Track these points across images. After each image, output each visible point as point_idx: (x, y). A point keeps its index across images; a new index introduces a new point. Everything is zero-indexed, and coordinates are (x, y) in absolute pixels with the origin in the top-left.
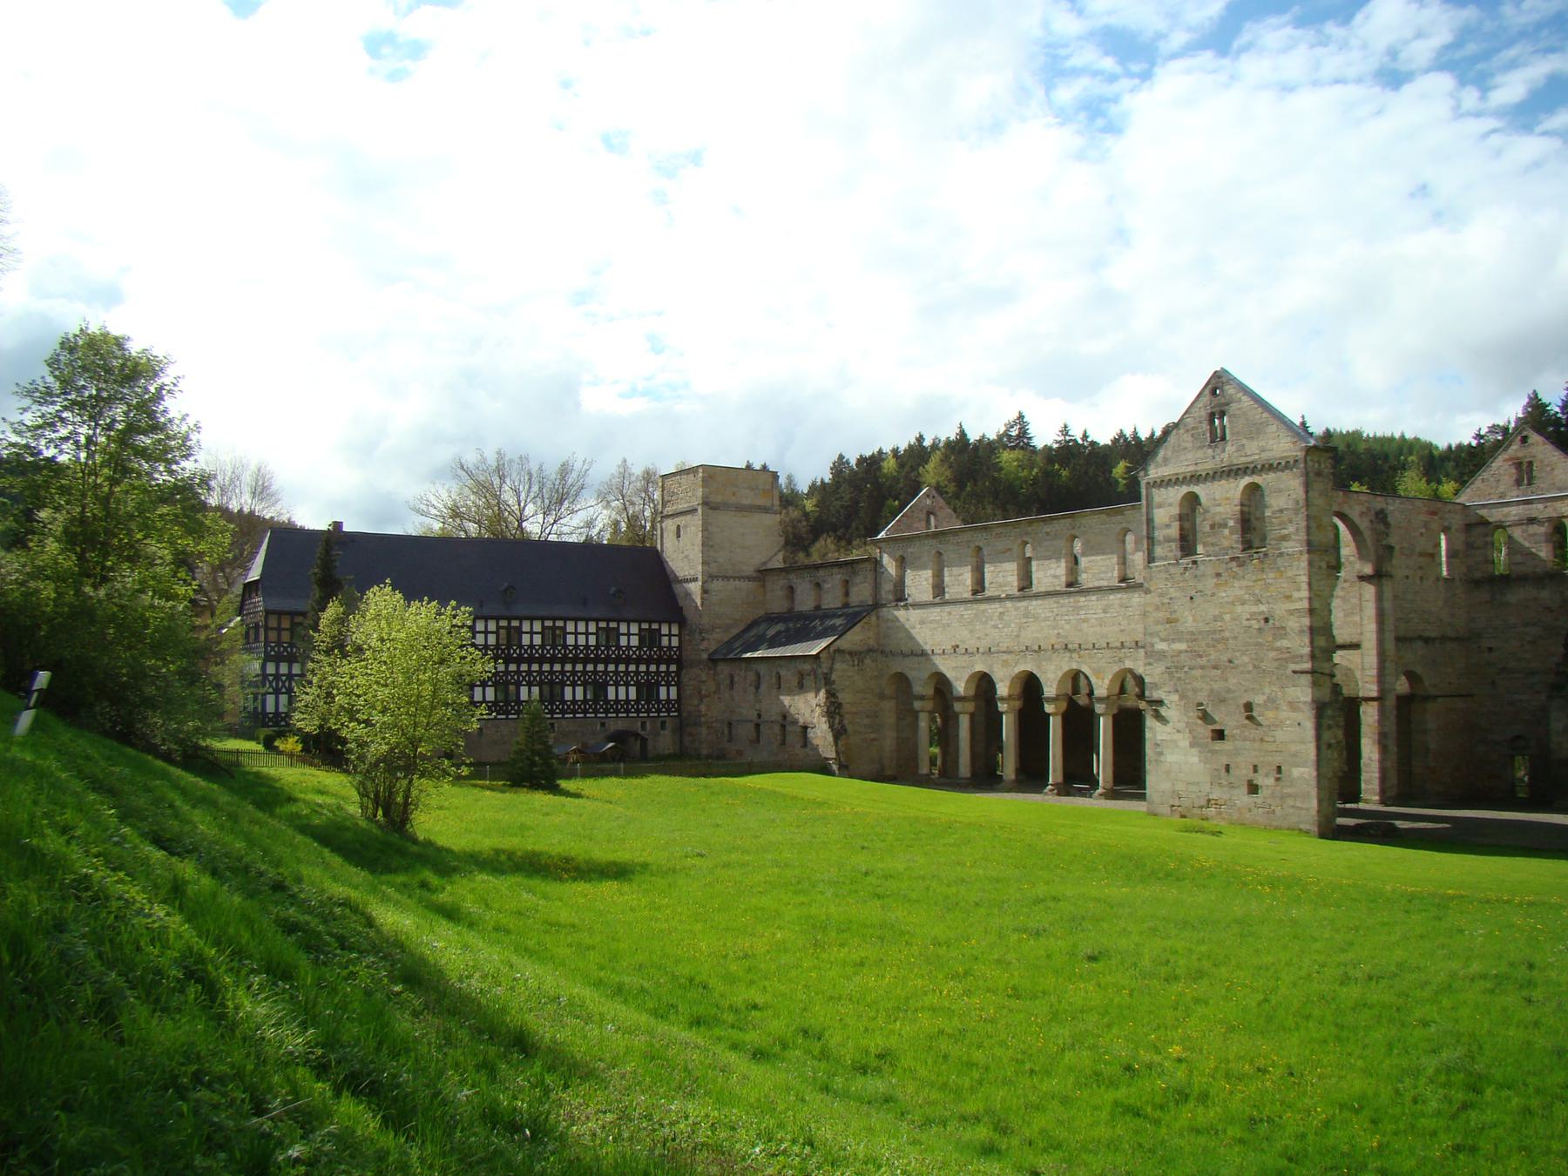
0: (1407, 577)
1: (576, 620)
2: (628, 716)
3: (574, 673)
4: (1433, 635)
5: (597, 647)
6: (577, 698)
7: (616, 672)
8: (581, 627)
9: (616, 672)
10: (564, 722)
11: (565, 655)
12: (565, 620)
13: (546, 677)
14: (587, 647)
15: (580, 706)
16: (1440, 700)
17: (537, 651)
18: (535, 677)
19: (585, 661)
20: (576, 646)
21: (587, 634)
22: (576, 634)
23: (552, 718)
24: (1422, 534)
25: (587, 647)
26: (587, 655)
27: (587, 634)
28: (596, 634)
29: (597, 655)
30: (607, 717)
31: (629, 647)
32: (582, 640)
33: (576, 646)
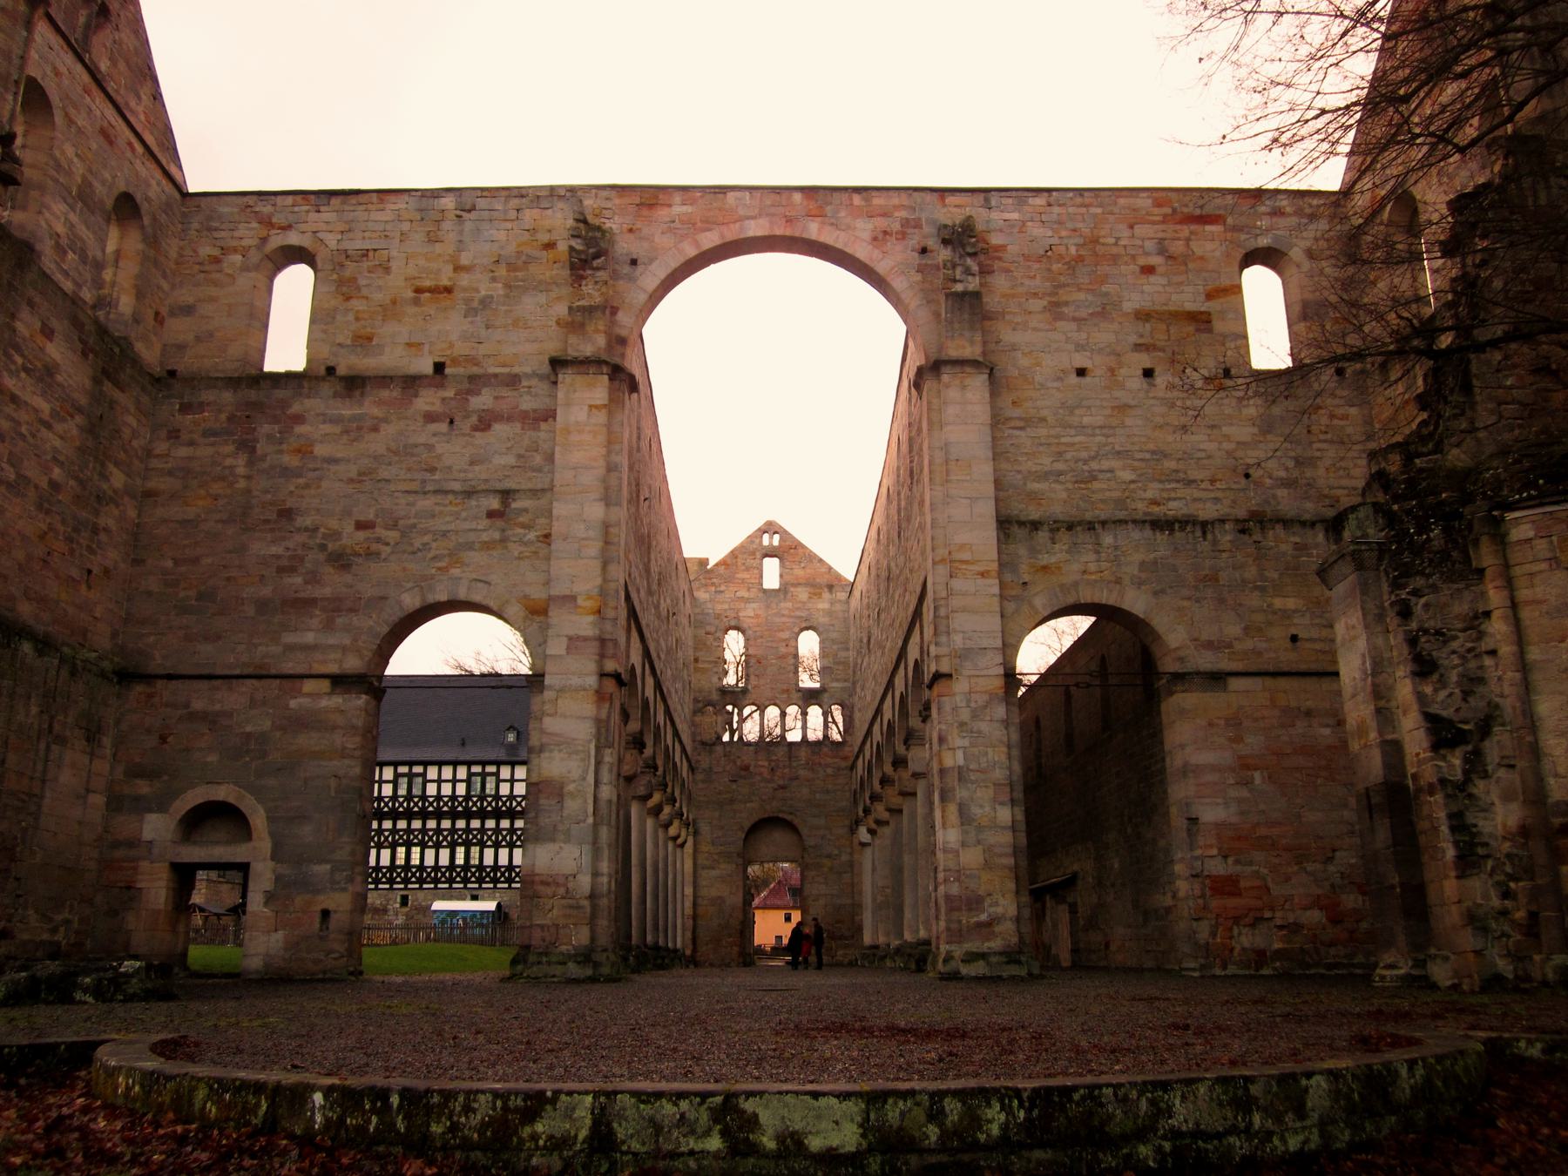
0: (1081, 372)
1: (440, 764)
2: (510, 887)
3: (438, 831)
4: (1208, 512)
5: (468, 797)
6: (441, 864)
7: (497, 830)
8: (447, 772)
9: (497, 830)
10: (421, 895)
11: (424, 808)
12: (426, 764)
13: (401, 837)
14: (453, 797)
15: (443, 874)
16: (1235, 684)
17: (386, 804)
18: (386, 838)
19: (454, 816)
20: (439, 797)
21: (454, 781)
22: (439, 781)
23: (406, 888)
24: (1148, 270)
25: (453, 797)
26: (453, 808)
27: (454, 781)
28: (468, 782)
29: (467, 809)
30: (480, 888)
31: (511, 797)
32: (447, 789)
33: (439, 797)
